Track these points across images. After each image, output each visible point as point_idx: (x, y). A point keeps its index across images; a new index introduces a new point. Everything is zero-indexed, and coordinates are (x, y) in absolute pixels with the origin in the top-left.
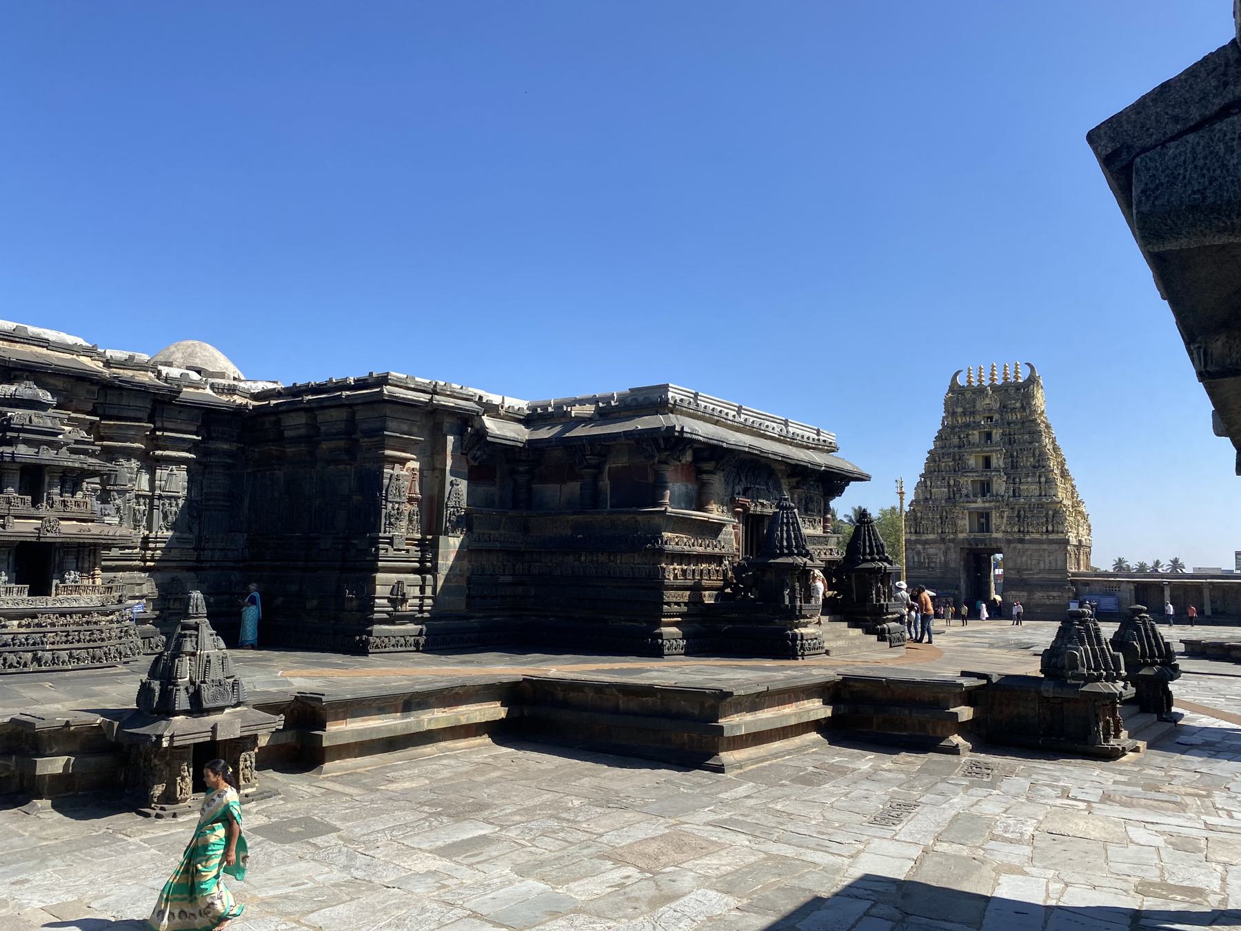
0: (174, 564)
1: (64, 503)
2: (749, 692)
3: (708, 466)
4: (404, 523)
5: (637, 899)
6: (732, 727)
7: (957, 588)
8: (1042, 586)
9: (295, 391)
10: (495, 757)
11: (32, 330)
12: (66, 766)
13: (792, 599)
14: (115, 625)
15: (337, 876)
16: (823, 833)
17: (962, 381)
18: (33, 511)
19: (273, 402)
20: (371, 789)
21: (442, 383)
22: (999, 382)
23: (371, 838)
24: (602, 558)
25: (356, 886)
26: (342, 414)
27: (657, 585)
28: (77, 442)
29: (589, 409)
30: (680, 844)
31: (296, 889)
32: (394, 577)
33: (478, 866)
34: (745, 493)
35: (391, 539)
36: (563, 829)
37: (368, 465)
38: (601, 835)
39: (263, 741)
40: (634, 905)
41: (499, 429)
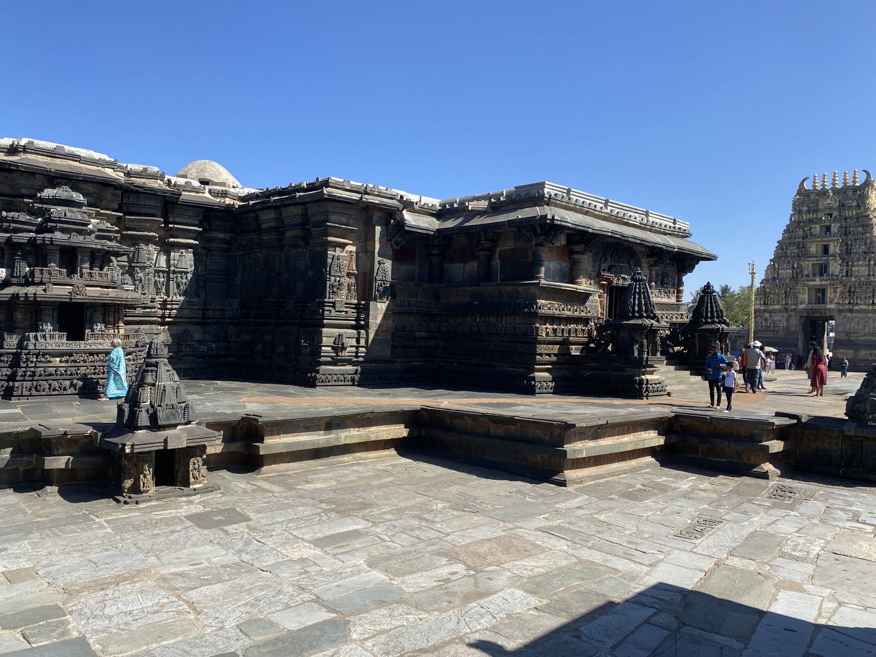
0: (186, 320)
1: (90, 275)
2: (590, 424)
3: (579, 248)
4: (344, 292)
5: (454, 594)
6: (575, 451)
7: (796, 346)
8: (866, 346)
9: (268, 194)
10: (394, 466)
11: (68, 149)
12: (67, 463)
13: (641, 352)
14: (132, 362)
15: (231, 558)
16: (632, 543)
17: (808, 186)
18: (68, 280)
19: (251, 202)
20: (290, 488)
21: (371, 186)
22: (839, 186)
23: (271, 528)
24: (492, 320)
25: (240, 568)
26: (296, 211)
27: (531, 340)
28: (99, 230)
29: (483, 204)
30: (512, 547)
31: (192, 568)
32: (336, 331)
33: (341, 557)
34: (609, 270)
35: (334, 303)
36: (419, 528)
37: (317, 249)
38: (448, 535)
39: (210, 450)
40: (450, 599)
41: (415, 221)
